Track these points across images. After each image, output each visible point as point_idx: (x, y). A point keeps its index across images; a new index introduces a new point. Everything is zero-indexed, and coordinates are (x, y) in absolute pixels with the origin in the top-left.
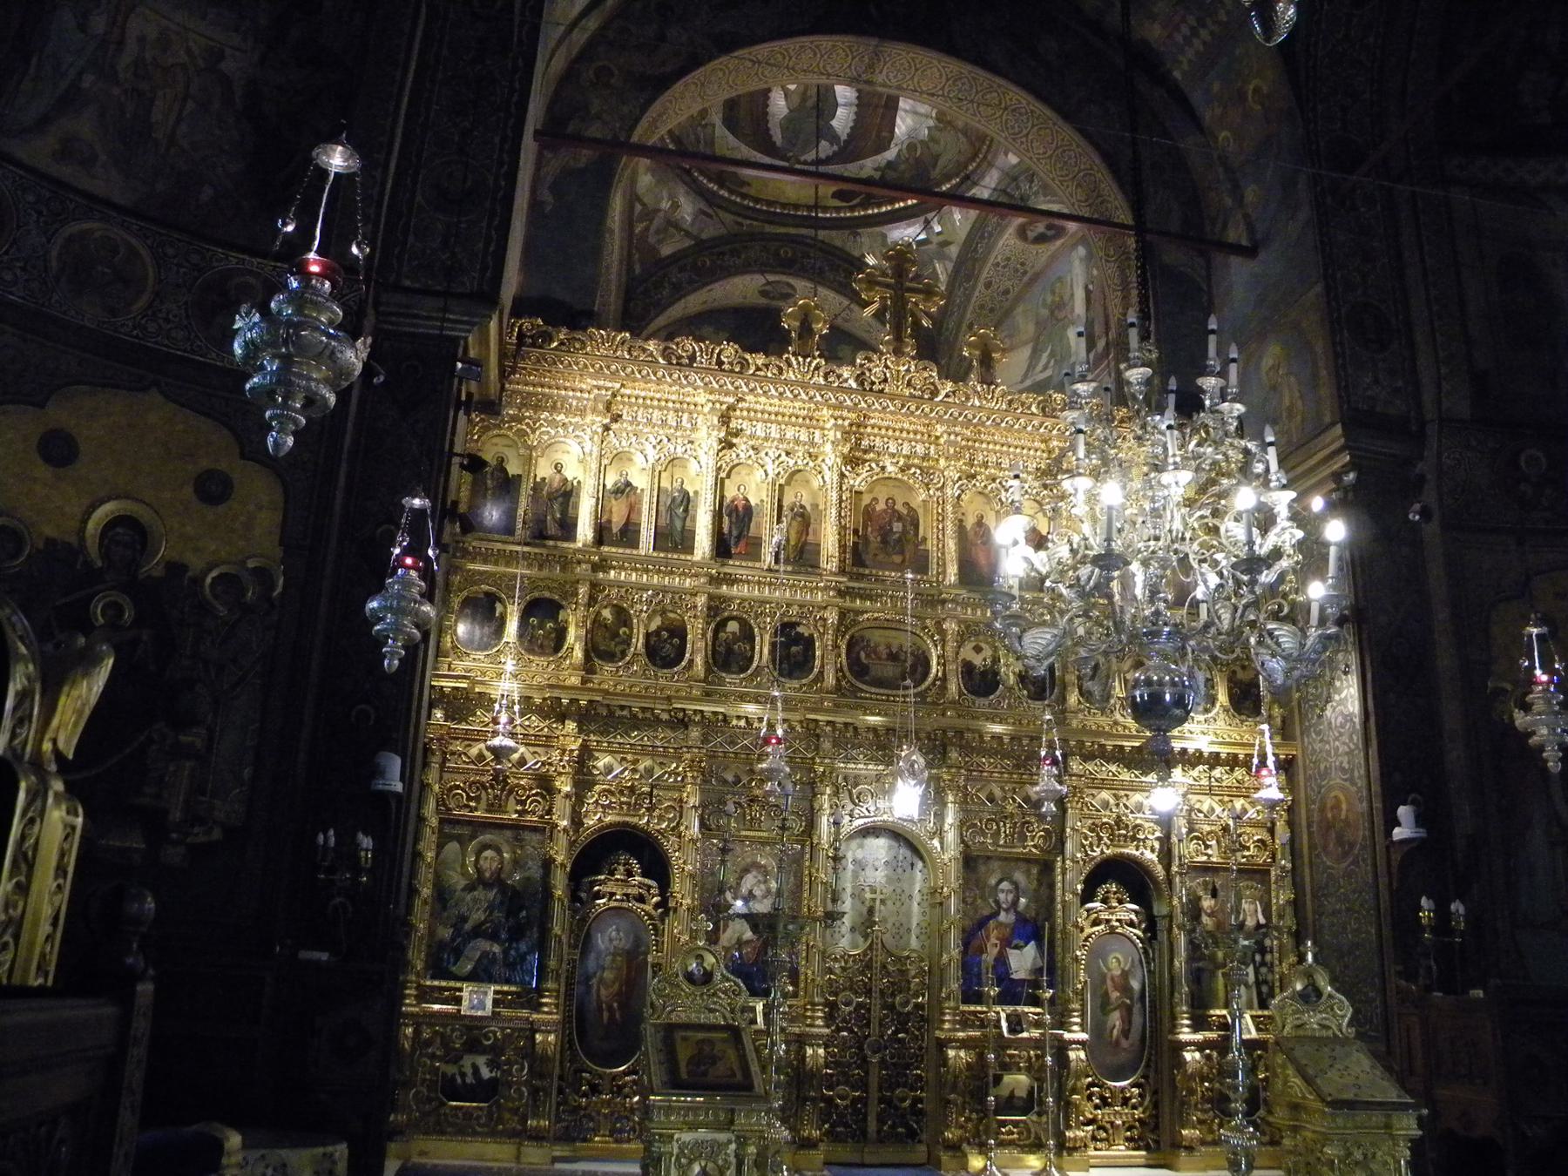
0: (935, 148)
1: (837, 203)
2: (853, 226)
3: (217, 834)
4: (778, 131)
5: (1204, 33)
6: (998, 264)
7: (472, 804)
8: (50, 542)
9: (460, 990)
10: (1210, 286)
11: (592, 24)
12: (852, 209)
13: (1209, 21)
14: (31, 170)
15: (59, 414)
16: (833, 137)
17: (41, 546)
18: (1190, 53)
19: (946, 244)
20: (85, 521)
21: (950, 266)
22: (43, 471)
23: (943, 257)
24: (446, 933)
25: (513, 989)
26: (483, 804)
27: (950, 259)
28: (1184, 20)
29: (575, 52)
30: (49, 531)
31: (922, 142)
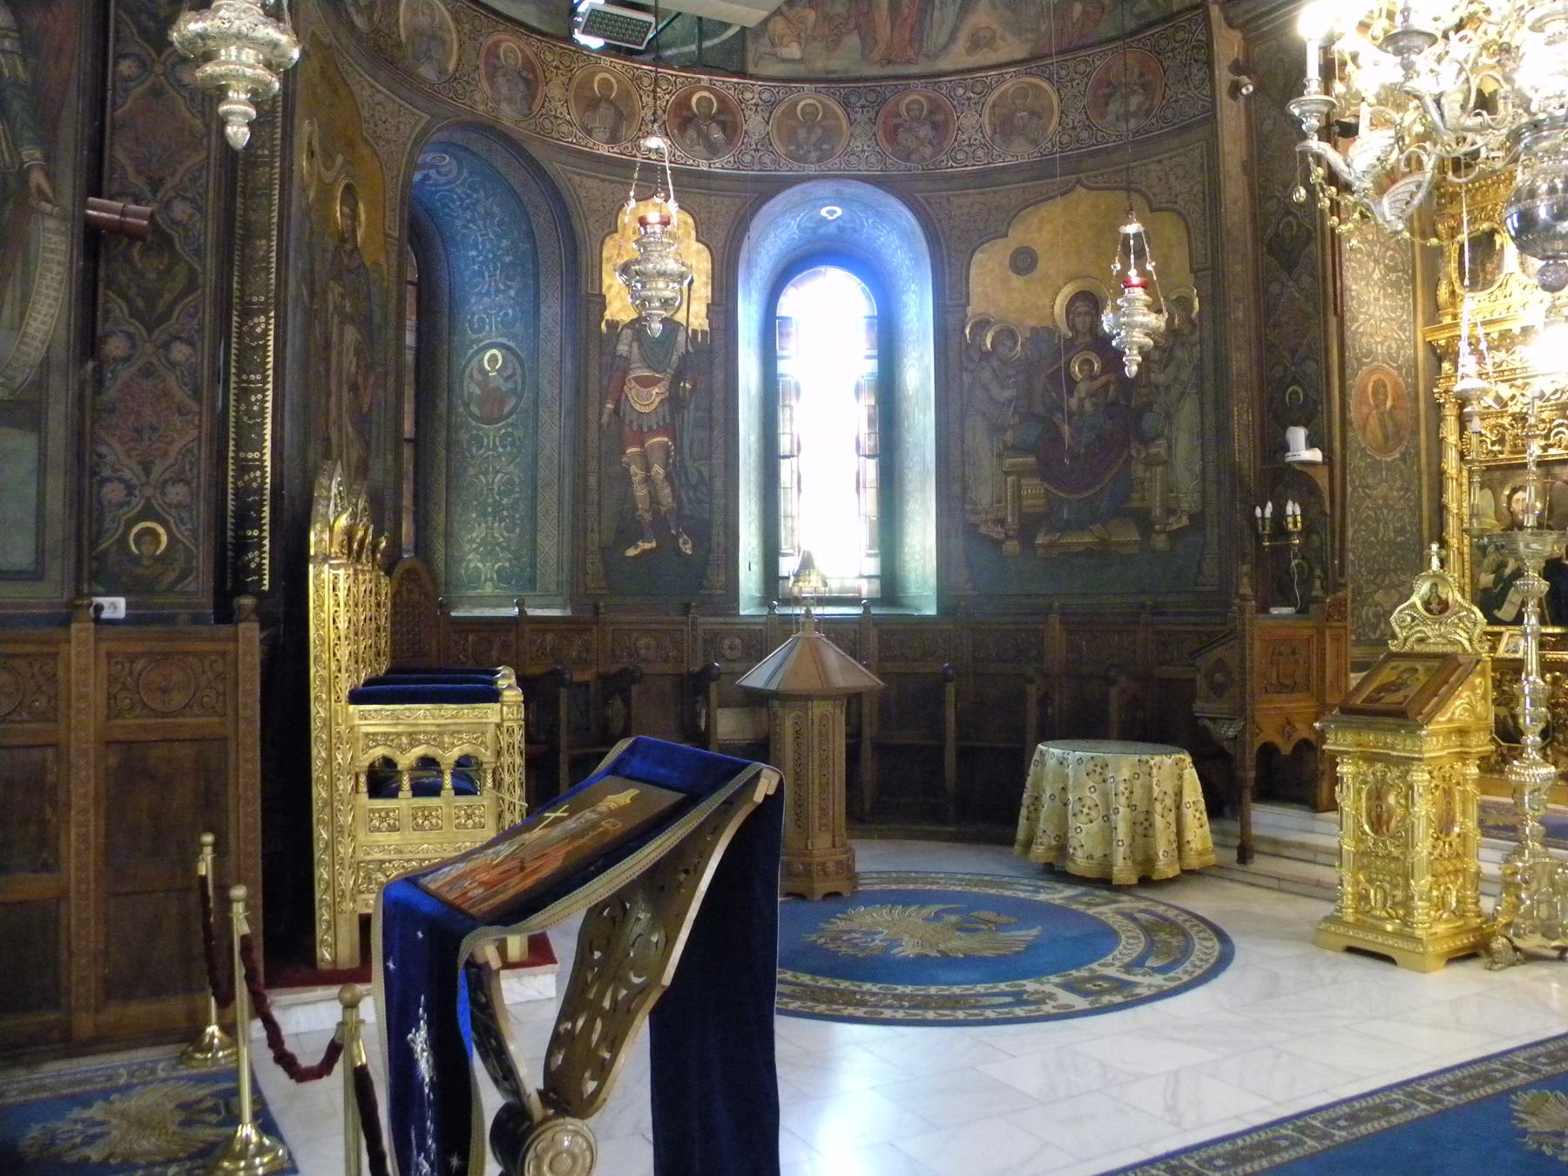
3: (1185, 521)
7: (1496, 448)
8: (1034, 330)
9: (1501, 634)
14: (956, 72)
15: (1018, 236)
17: (1028, 335)
20: (1052, 307)
22: (1017, 281)
24: (1487, 579)
25: (1557, 630)
26: (1508, 448)
30: (1033, 323)
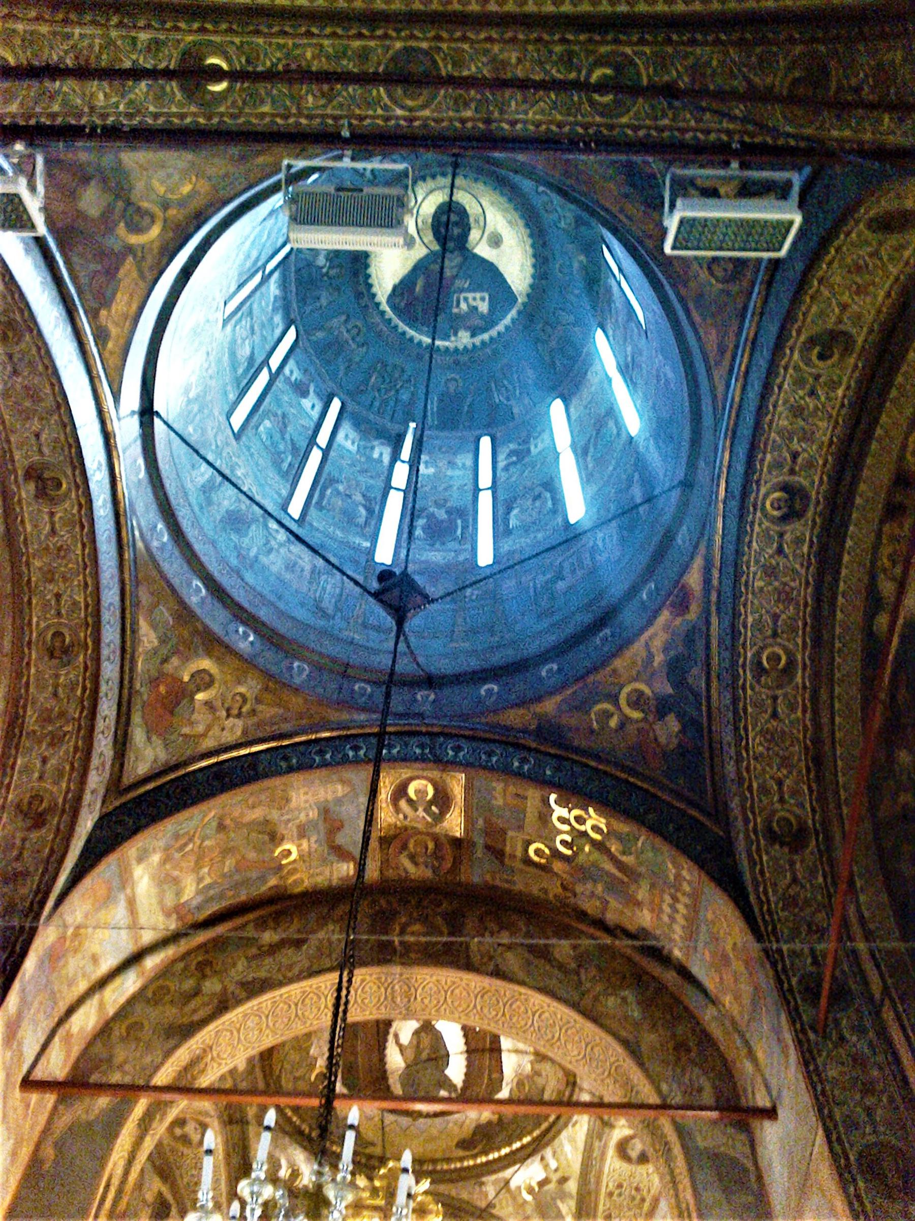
0: (540, 1081)
1: (461, 1153)
2: (478, 1173)
4: (399, 1086)
5: (680, 907)
6: (611, 1194)
10: (756, 1163)
11: (130, 983)
12: (474, 1157)
13: (679, 895)
16: (451, 1086)
18: (678, 929)
19: (563, 1180)
21: (572, 1203)
23: (563, 1196)
27: (571, 1196)
28: (662, 901)
29: (111, 1011)
31: (528, 1077)
